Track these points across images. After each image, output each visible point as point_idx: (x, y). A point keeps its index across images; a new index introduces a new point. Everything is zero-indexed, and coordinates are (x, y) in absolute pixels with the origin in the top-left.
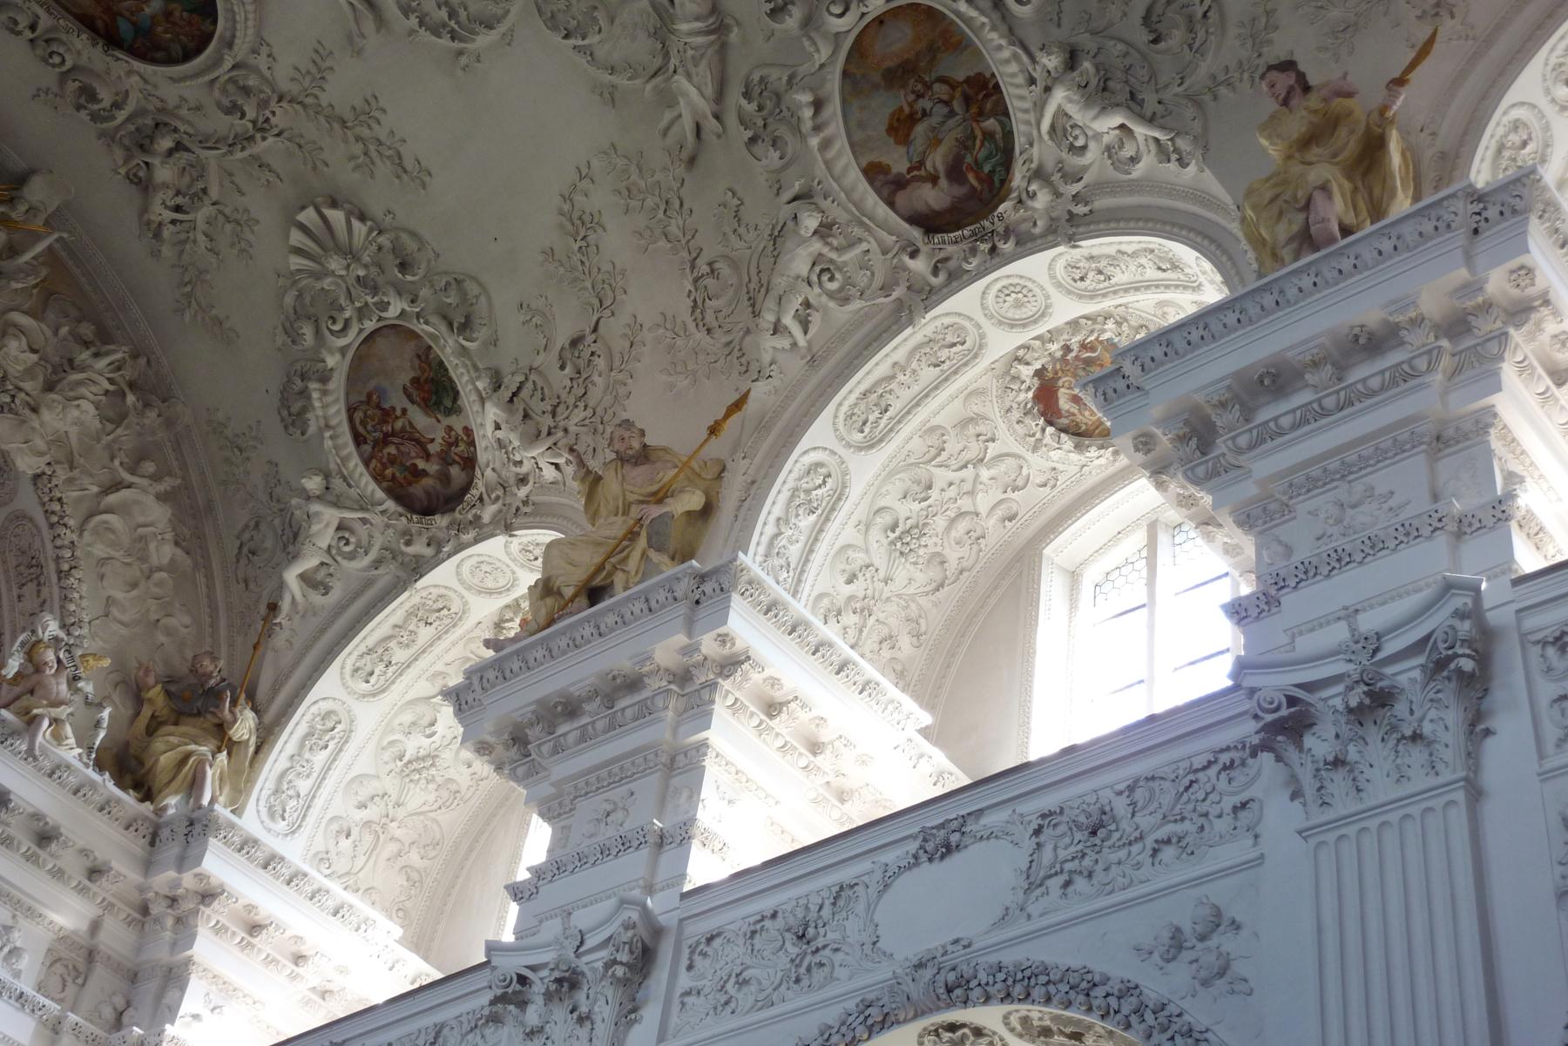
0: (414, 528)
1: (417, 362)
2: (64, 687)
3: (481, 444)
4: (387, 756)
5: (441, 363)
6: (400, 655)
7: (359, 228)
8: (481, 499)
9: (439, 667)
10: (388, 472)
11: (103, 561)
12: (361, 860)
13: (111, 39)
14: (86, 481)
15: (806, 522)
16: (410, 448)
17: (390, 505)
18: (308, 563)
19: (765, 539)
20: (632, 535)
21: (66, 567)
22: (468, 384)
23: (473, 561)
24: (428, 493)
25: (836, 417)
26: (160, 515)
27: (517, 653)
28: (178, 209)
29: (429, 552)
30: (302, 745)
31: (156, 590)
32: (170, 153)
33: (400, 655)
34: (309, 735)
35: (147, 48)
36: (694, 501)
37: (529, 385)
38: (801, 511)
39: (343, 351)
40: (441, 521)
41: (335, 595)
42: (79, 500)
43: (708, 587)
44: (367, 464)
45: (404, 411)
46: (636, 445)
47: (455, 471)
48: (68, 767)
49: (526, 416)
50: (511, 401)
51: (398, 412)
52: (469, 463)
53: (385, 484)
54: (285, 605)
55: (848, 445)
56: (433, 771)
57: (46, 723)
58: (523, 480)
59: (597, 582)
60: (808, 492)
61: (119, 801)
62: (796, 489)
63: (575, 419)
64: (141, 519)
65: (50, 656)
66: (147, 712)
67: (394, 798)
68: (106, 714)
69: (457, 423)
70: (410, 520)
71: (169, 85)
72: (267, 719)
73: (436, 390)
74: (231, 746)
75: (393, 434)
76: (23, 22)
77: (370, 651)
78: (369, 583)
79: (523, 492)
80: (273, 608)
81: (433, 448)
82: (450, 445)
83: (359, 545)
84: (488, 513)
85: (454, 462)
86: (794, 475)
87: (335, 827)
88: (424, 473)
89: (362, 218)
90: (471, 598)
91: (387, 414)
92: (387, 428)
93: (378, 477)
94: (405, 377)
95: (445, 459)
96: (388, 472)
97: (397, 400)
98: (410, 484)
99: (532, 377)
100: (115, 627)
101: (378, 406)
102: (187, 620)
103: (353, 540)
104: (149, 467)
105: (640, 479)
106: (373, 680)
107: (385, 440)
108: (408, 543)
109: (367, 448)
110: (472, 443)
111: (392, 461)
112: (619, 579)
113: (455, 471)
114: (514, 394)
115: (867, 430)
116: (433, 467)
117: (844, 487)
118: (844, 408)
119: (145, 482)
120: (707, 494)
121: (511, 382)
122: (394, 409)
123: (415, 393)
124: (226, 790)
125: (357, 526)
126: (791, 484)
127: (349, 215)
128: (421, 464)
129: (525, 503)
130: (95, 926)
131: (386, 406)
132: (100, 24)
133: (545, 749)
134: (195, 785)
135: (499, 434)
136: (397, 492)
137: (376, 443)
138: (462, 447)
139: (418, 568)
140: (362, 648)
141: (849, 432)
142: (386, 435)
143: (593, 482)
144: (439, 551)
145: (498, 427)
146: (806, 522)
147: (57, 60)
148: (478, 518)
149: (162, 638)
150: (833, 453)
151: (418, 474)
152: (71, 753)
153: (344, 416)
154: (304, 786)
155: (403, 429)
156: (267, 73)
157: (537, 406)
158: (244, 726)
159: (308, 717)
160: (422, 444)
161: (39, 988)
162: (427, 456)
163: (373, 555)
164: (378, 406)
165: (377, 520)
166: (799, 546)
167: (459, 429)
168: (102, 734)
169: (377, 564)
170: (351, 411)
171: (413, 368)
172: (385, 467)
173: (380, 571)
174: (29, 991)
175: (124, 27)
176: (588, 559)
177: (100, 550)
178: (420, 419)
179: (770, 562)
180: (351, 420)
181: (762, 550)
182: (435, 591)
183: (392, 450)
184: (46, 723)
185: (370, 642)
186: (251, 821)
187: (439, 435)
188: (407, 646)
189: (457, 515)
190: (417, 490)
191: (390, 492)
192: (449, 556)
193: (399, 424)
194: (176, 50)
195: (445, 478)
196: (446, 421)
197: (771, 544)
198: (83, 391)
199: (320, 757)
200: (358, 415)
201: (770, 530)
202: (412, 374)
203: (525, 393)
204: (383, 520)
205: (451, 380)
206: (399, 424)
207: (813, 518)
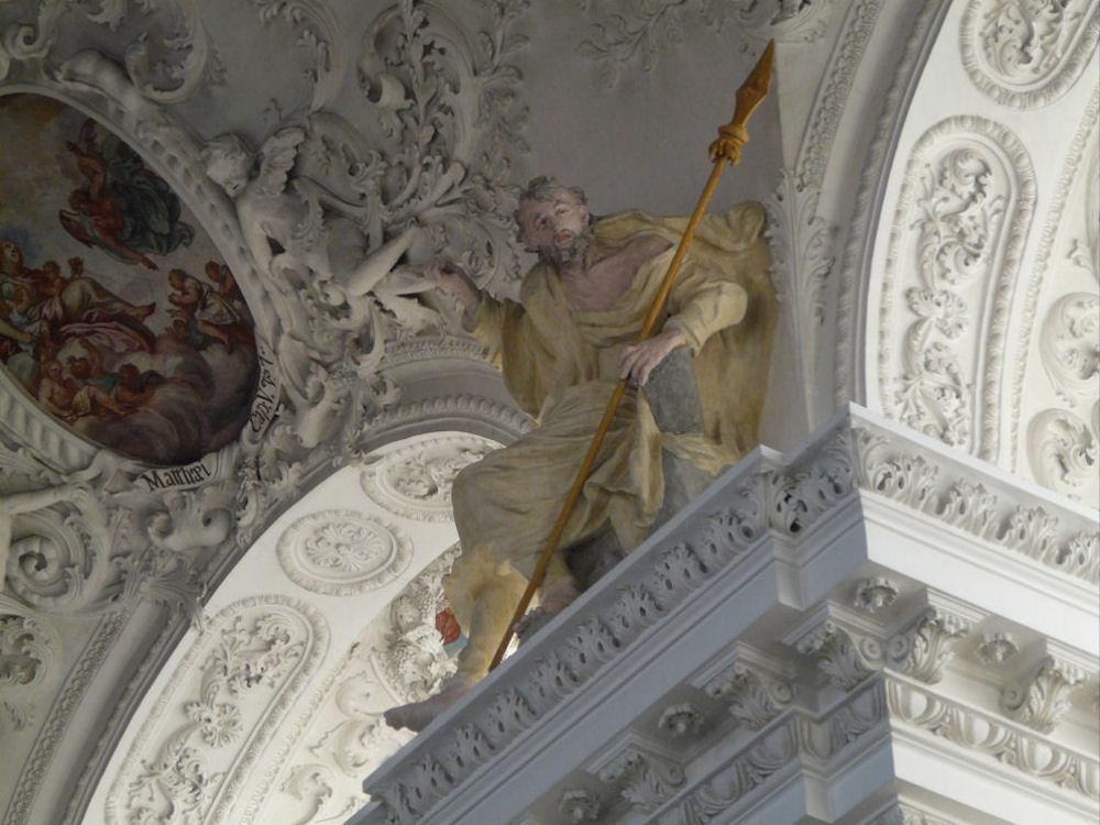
0: (170, 495)
1: (73, 159)
3: (251, 292)
5: (123, 150)
6: (214, 760)
8: (287, 402)
9: (299, 758)
10: (82, 397)
15: (967, 282)
16: (119, 339)
17: (107, 460)
19: (894, 345)
20: (621, 416)
22: (193, 177)
23: (304, 532)
24: (171, 416)
25: (964, 47)
27: (458, 722)
33: (214, 760)
36: (723, 307)
38: (949, 262)
40: (218, 465)
41: (52, 673)
43: (807, 491)
45: (76, 265)
47: (215, 357)
49: (329, 213)
50: (288, 188)
51: (66, 272)
52: (241, 333)
53: (81, 424)
55: (1007, 98)
58: (363, 343)
59: (575, 532)
60: (951, 218)
62: (925, 223)
69: (189, 260)
70: (154, 483)
73: (127, 205)
75: (69, 317)
78: (110, 632)
79: (369, 365)
81: (157, 324)
82: (189, 309)
83: (67, 563)
84: (310, 428)
85: (208, 341)
86: (916, 191)
88: (155, 379)
90: (320, 604)
91: (44, 282)
92: (53, 309)
93: (64, 412)
94: (57, 197)
95: (188, 338)
96: (82, 397)
97: (56, 248)
98: (132, 408)
101: (21, 270)
103: (51, 553)
107: (56, 335)
110: (235, 293)
111: (83, 372)
112: (618, 511)
113: (215, 357)
114: (292, 175)
115: (1035, 52)
116: (168, 363)
117: (1022, 184)
118: (977, 25)
120: (747, 283)
121: (280, 151)
122: (54, 266)
123: (88, 224)
125: (51, 522)
126: (913, 213)
128: (143, 363)
129: (380, 387)
131: (37, 264)
135: (283, 261)
136: (112, 431)
137: (39, 344)
138: (215, 307)
139: (197, 580)
140: (136, 768)
141: (1001, 68)
142: (55, 323)
144: (232, 530)
145: (276, 248)
146: (967, 282)
150: (979, 122)
155: (85, 300)
160: (131, 322)
162: (150, 343)
163: (103, 571)
164: (21, 270)
165: (86, 501)
166: (968, 333)
169: (116, 587)
171: (67, 173)
172: (71, 389)
176: (538, 493)
178: (113, 273)
179: (914, 383)
182: (249, 613)
183: (75, 350)
185: (148, 750)
187: (162, 295)
188: (225, 736)
189: (246, 443)
191: (97, 436)
192: (257, 534)
193: (73, 295)
195: (199, 377)
196: (167, 263)
197: (907, 349)
201: (899, 320)
202: (70, 186)
204: (99, 498)
205: (152, 177)
206: (73, 295)
207: (977, 268)
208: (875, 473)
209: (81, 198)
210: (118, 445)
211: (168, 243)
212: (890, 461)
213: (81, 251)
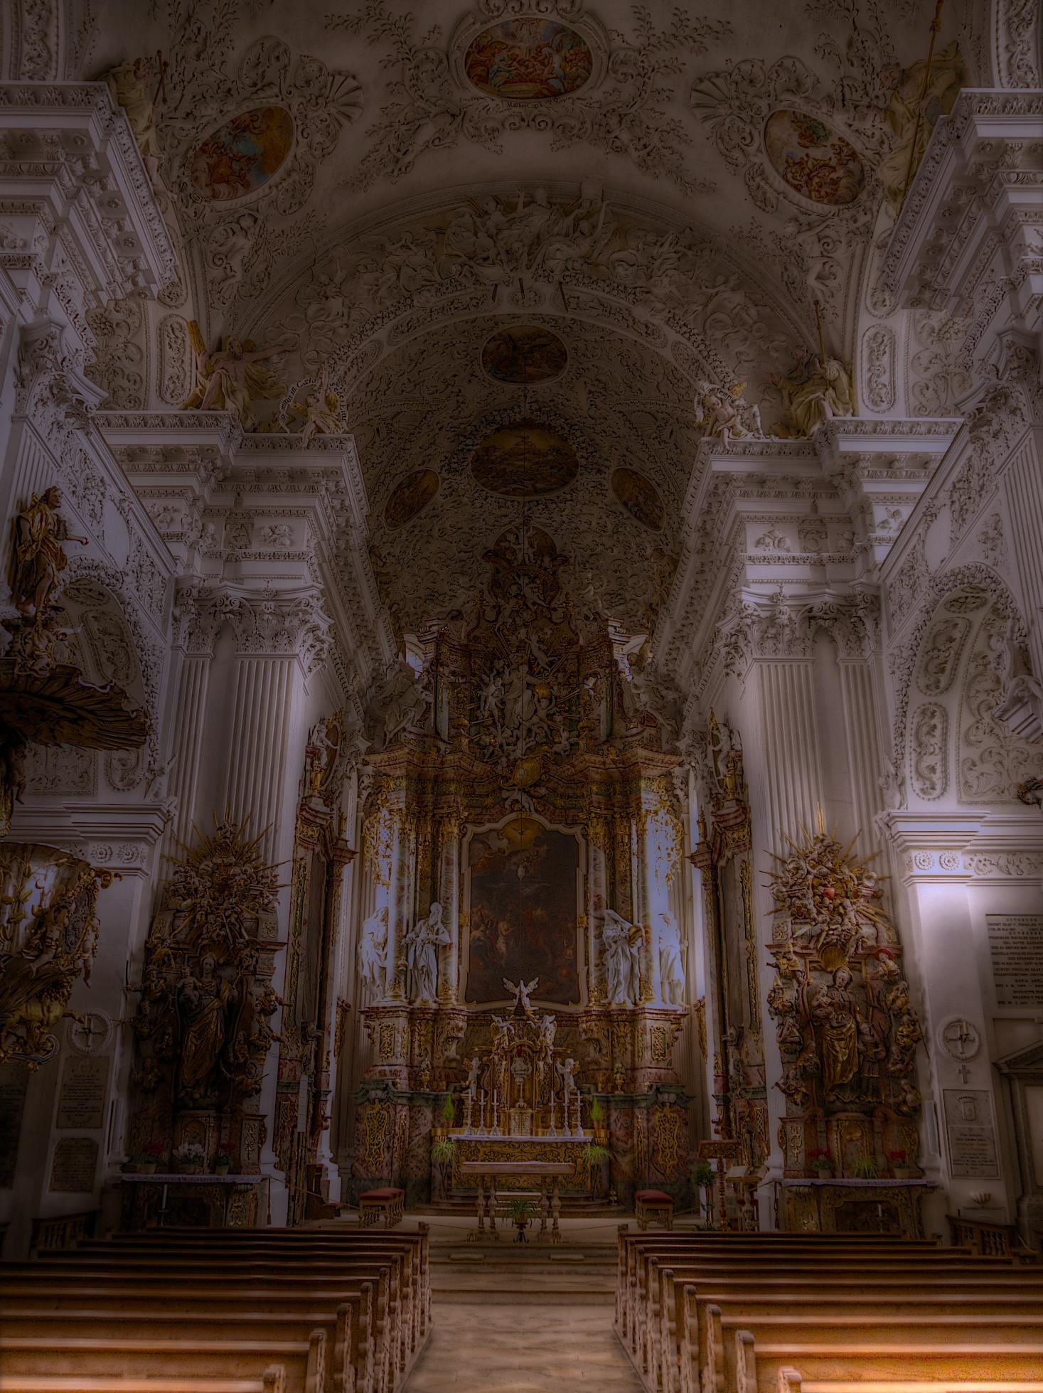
2: (730, 410)
4: (925, 335)
7: (718, 81)
10: (823, 193)
11: (723, 340)
12: (943, 396)
13: (556, 94)
14: (694, 307)
16: (825, 171)
18: (816, 268)
21: (705, 354)
22: (820, 114)
26: (738, 298)
27: (894, 240)
28: (645, 146)
29: (868, 217)
30: (870, 360)
31: (758, 334)
32: (620, 122)
34: (872, 352)
35: (572, 84)
37: (847, 89)
38: (1020, 29)
39: (759, 150)
42: (695, 319)
43: (958, 125)
44: (810, 197)
45: (807, 155)
46: (896, 74)
47: (851, 165)
48: (750, 444)
52: (853, 155)
54: (820, 297)
56: (956, 326)
57: (726, 431)
61: (786, 445)
63: (877, 87)
64: (732, 306)
65: (714, 399)
66: (785, 394)
67: (943, 355)
68: (756, 408)
69: (833, 140)
71: (596, 91)
72: (847, 358)
74: (832, 384)
76: (517, 121)
77: (875, 290)
78: (853, 256)
80: (817, 303)
81: (833, 163)
87: (917, 389)
89: (717, 75)
91: (801, 164)
93: (820, 200)
94: (795, 139)
95: (842, 164)
96: (823, 193)
97: (800, 153)
99: (845, 83)
100: (746, 365)
102: (784, 338)
104: (721, 279)
105: (909, 92)
106: (887, 303)
108: (855, 222)
109: (805, 189)
110: (848, 144)
119: (722, 288)
124: (840, 406)
127: (709, 79)
128: (834, 176)
130: (815, 508)
131: (797, 160)
132: (546, 92)
133: (940, 279)
134: (821, 413)
138: (845, 150)
140: (870, 291)
142: (808, 175)
143: (889, 113)
147: (543, 125)
148: (877, 180)
149: (774, 355)
151: (835, 182)
152: (749, 437)
153: (783, 183)
154: (885, 379)
156: (625, 45)
157: (856, 96)
158: (833, 369)
159: (865, 345)
161: (804, 550)
162: (834, 169)
167: (837, 142)
168: (759, 419)
169: (849, 244)
170: (784, 177)
173: (854, 244)
174: (797, 554)
175: (555, 83)
177: (719, 335)
178: (817, 153)
179: (1015, 76)
180: (787, 181)
181: (1004, 74)
183: (816, 180)
184: (726, 431)
186: (866, 414)
187: (831, 153)
190: (842, 191)
191: (830, 202)
194: (581, 71)
195: (850, 173)
196: (829, 144)
198: (665, 267)
199: (886, 358)
200: (789, 175)
203: (848, 95)
208: (975, 108)
209: (801, 136)
210: (836, 203)
211: (826, 137)
212: (981, 101)
213: (807, 151)
